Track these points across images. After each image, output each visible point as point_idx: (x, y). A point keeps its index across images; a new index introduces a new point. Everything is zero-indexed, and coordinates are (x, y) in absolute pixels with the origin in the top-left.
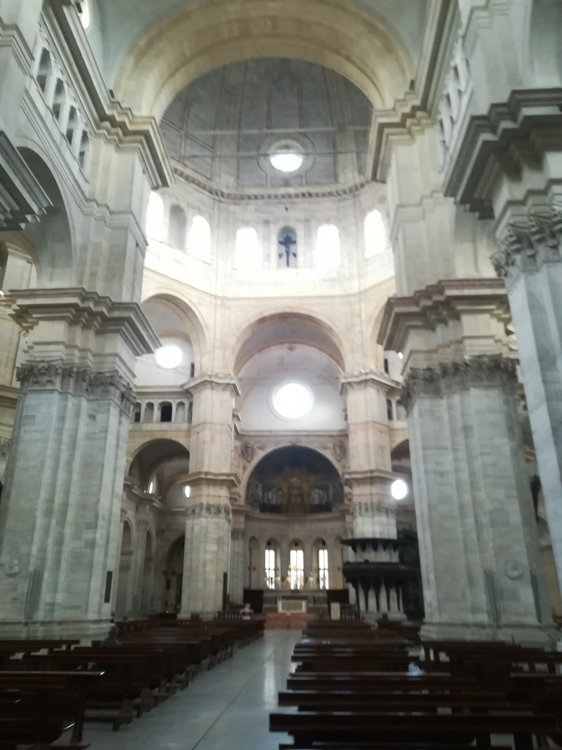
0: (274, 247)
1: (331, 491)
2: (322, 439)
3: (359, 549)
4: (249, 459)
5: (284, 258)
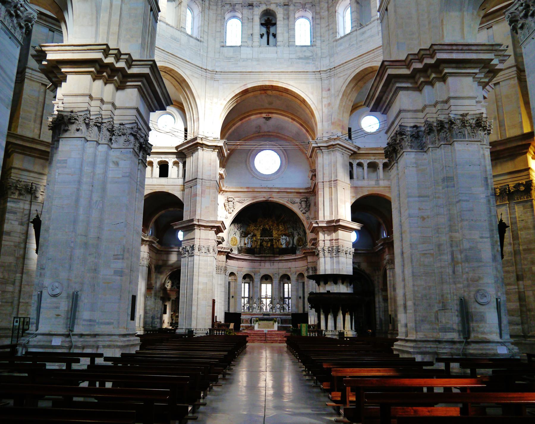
0: (257, 29)
1: (296, 238)
2: (291, 196)
3: (322, 283)
5: (265, 37)
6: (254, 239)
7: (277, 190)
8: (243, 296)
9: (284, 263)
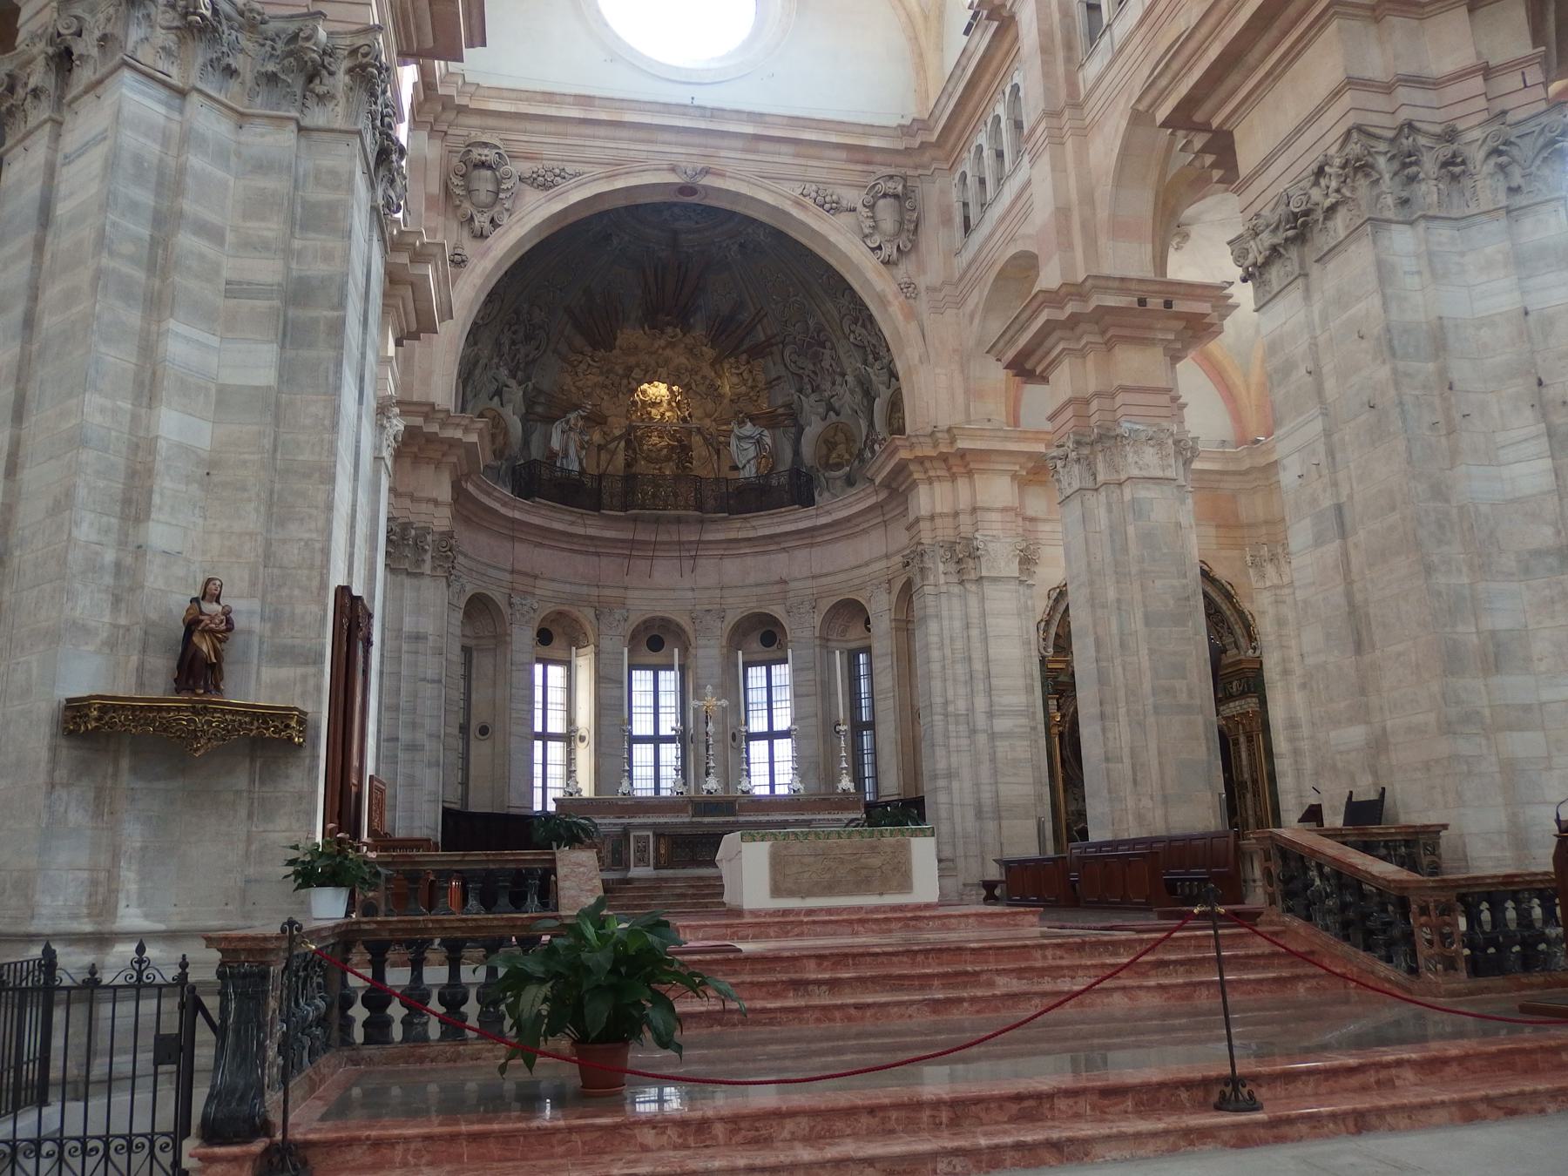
1: (813, 430)
4: (481, 220)
6: (597, 437)
7: (749, 129)
8: (538, 728)
9: (750, 561)
